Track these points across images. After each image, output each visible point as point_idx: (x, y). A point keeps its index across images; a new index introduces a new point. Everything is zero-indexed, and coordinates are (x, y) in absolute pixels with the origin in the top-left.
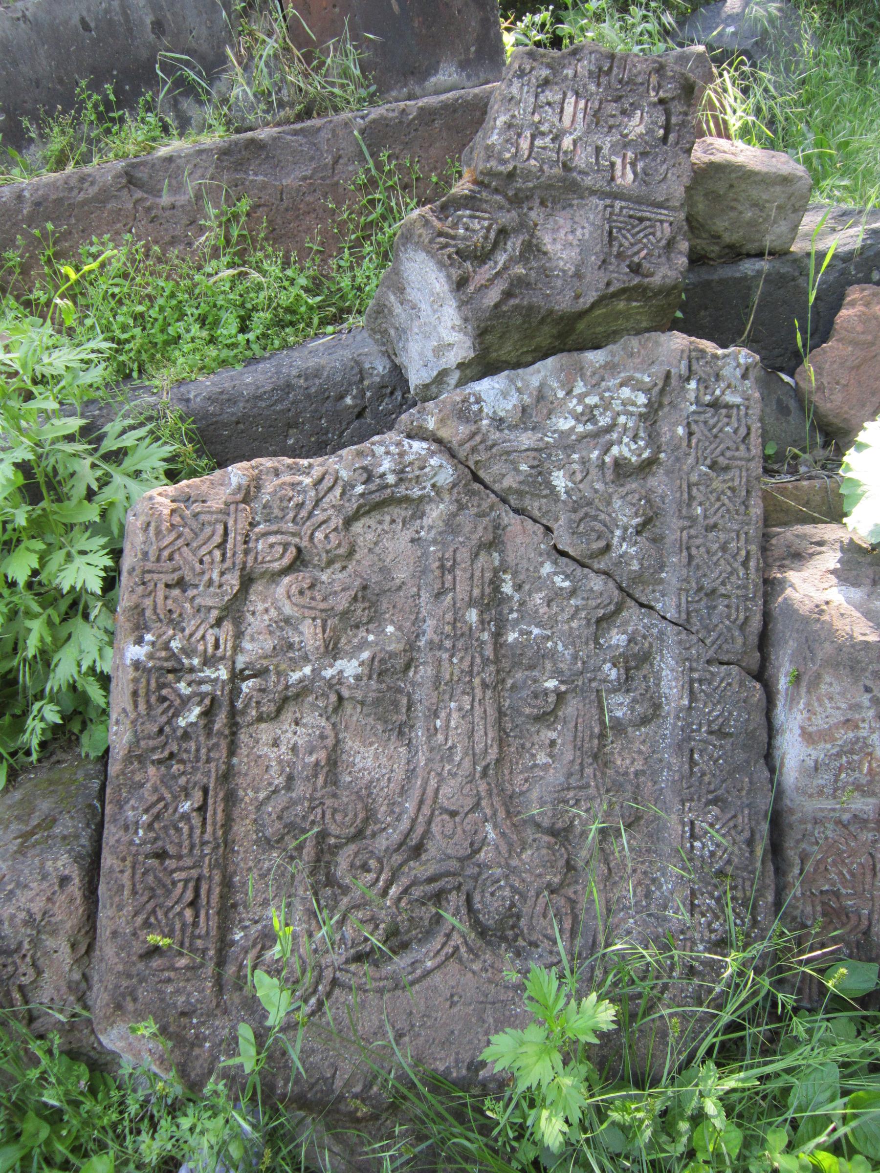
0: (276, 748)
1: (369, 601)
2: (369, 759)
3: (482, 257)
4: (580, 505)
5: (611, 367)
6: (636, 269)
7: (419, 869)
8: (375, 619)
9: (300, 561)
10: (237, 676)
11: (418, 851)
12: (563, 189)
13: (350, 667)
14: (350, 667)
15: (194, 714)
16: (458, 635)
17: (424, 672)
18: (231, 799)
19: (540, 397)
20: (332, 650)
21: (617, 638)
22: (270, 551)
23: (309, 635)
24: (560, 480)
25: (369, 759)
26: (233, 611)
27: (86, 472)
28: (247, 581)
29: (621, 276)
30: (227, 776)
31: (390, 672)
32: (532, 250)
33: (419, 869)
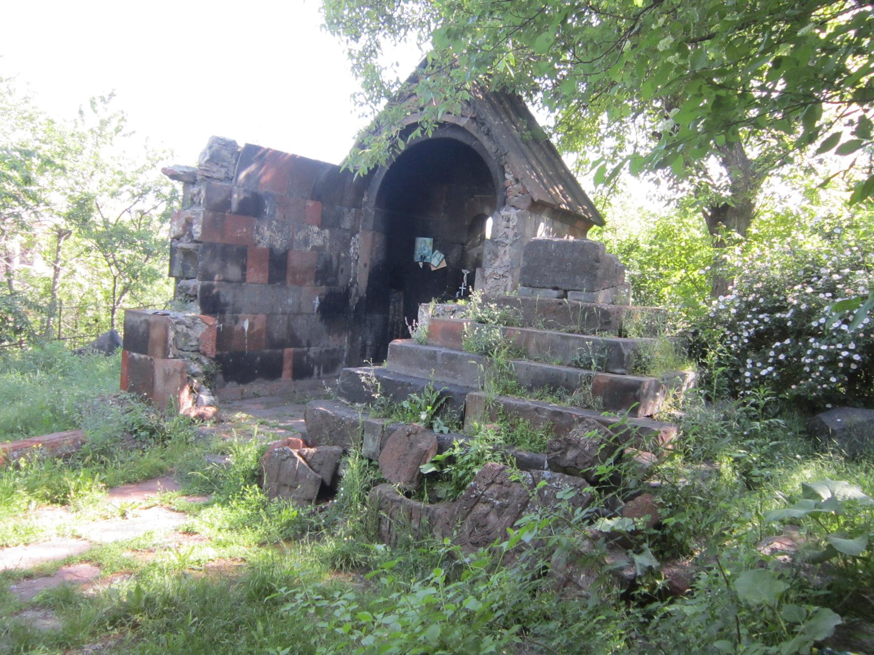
0: (482, 508)
1: (507, 495)
2: (492, 518)
3: (555, 450)
5: (569, 479)
6: (576, 464)
7: (487, 537)
8: (506, 498)
9: (502, 483)
10: (482, 494)
11: (489, 534)
12: (576, 445)
13: (498, 502)
14: (498, 502)
15: (473, 496)
16: (516, 507)
17: (507, 510)
18: (471, 511)
19: (554, 478)
20: (497, 499)
23: (495, 495)
24: (546, 492)
25: (492, 518)
26: (488, 485)
27: (488, 456)
28: (493, 482)
29: (572, 464)
30: (472, 507)
31: (503, 506)
32: (564, 453)
33: (487, 537)
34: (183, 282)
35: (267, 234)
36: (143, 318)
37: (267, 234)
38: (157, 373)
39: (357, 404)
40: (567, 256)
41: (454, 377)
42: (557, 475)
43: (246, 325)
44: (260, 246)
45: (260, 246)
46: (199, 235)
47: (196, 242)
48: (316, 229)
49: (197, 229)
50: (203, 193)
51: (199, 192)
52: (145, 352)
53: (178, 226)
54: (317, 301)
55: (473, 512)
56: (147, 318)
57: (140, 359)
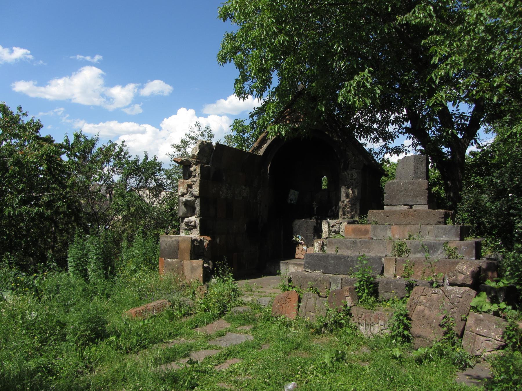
4: (452, 299)
21: (452, 310)
22: (424, 294)
34: (186, 220)
35: (225, 191)
36: (173, 239)
37: (225, 191)
38: (185, 268)
39: (317, 271)
40: (410, 188)
41: (368, 252)
42: (452, 288)
43: (218, 241)
44: (222, 197)
45: (222, 197)
46: (197, 193)
47: (196, 197)
48: (244, 187)
49: (196, 190)
50: (198, 170)
51: (195, 170)
52: (176, 257)
53: (183, 188)
54: (245, 226)
55: (416, 311)
56: (177, 238)
57: (173, 262)
